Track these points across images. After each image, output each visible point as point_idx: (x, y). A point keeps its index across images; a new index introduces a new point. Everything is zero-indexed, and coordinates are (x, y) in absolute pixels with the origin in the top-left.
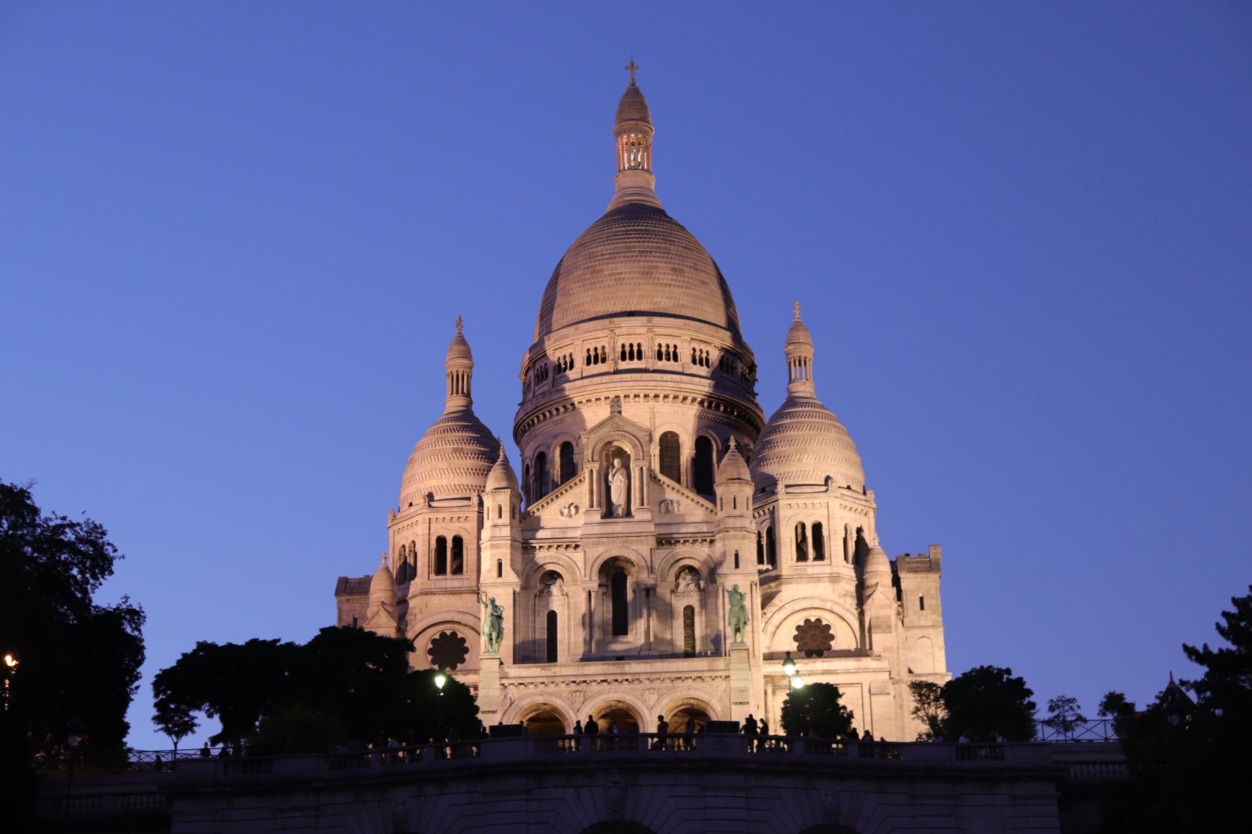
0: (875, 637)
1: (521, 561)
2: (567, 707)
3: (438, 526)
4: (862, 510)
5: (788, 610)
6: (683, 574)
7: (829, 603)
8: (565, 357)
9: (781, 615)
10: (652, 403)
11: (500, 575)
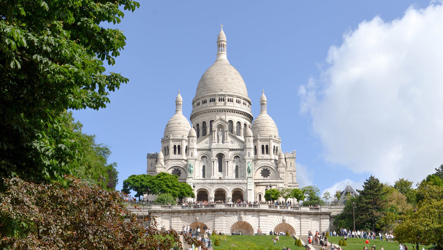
0: (280, 174)
3: (174, 143)
5: (260, 166)
9: (258, 168)
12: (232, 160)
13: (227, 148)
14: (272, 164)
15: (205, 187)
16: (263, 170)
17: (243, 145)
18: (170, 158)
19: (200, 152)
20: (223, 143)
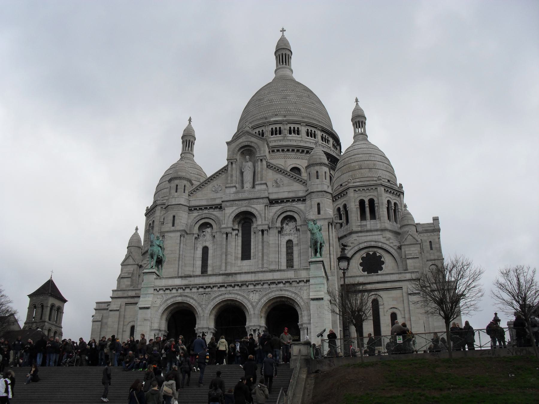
1: (186, 216)
2: (196, 304)
4: (397, 194)
5: (356, 248)
6: (286, 222)
7: (380, 243)
9: (353, 252)
10: (285, 153)
11: (173, 225)
13: (262, 197)
15: (188, 299)
16: (365, 255)
17: (306, 189)
19: (195, 214)
20: (253, 187)
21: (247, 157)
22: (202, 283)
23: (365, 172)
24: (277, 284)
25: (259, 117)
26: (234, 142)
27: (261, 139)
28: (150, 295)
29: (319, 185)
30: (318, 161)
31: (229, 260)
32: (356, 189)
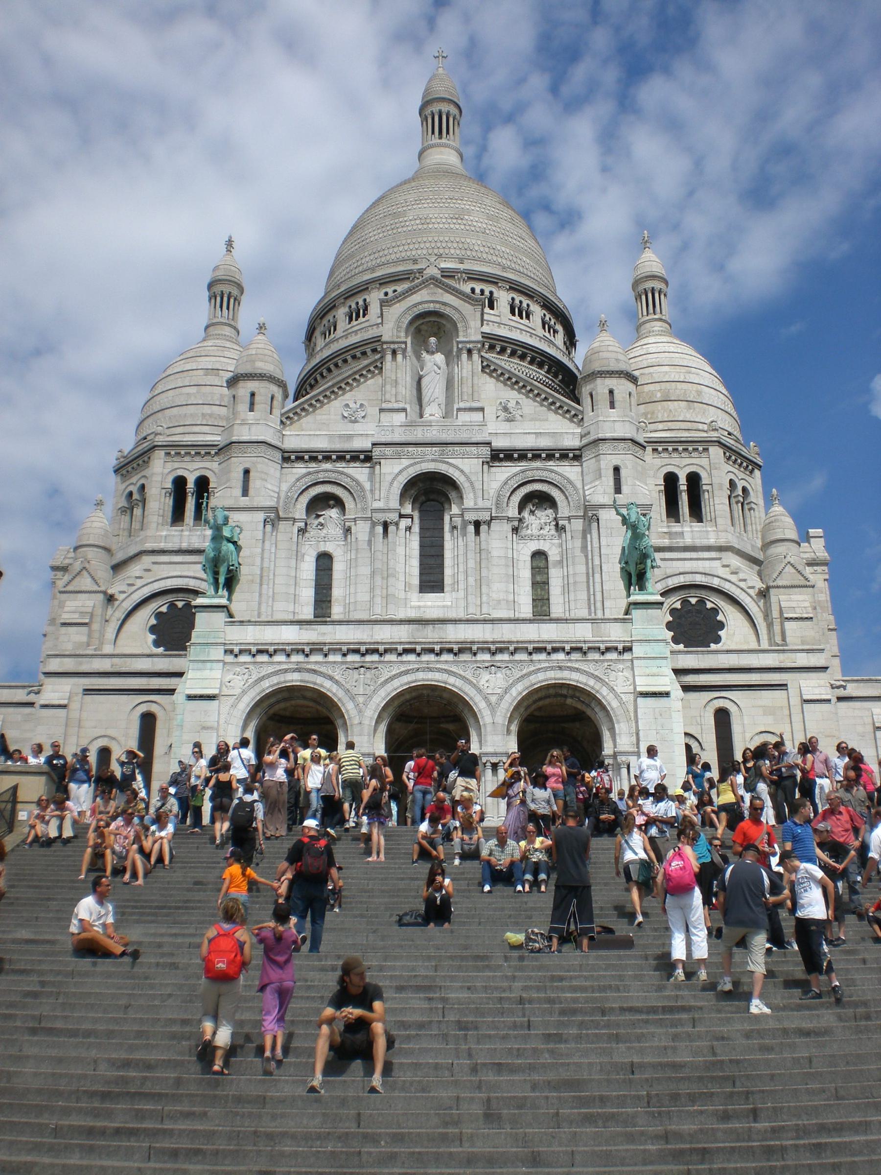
1: (278, 474)
2: (341, 693)
3: (176, 465)
4: (747, 466)
6: (530, 506)
7: (715, 578)
8: (357, 303)
11: (245, 492)
12: (509, 519)
13: (474, 440)
14: (732, 573)
15: (319, 680)
16: (678, 605)
18: (149, 546)
19: (300, 469)
21: (433, 340)
22: (356, 641)
23: (680, 410)
24: (549, 654)
25: (393, 257)
26: (399, 301)
27: (470, 299)
28: (214, 665)
29: (617, 424)
30: (613, 366)
31: (391, 590)
32: (659, 446)
